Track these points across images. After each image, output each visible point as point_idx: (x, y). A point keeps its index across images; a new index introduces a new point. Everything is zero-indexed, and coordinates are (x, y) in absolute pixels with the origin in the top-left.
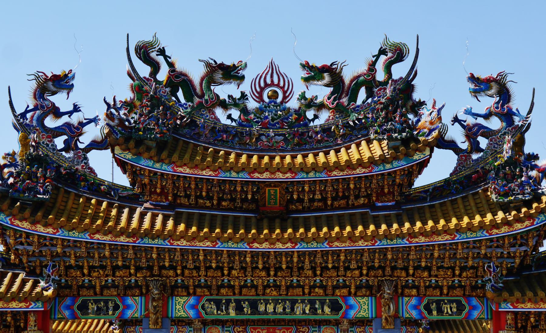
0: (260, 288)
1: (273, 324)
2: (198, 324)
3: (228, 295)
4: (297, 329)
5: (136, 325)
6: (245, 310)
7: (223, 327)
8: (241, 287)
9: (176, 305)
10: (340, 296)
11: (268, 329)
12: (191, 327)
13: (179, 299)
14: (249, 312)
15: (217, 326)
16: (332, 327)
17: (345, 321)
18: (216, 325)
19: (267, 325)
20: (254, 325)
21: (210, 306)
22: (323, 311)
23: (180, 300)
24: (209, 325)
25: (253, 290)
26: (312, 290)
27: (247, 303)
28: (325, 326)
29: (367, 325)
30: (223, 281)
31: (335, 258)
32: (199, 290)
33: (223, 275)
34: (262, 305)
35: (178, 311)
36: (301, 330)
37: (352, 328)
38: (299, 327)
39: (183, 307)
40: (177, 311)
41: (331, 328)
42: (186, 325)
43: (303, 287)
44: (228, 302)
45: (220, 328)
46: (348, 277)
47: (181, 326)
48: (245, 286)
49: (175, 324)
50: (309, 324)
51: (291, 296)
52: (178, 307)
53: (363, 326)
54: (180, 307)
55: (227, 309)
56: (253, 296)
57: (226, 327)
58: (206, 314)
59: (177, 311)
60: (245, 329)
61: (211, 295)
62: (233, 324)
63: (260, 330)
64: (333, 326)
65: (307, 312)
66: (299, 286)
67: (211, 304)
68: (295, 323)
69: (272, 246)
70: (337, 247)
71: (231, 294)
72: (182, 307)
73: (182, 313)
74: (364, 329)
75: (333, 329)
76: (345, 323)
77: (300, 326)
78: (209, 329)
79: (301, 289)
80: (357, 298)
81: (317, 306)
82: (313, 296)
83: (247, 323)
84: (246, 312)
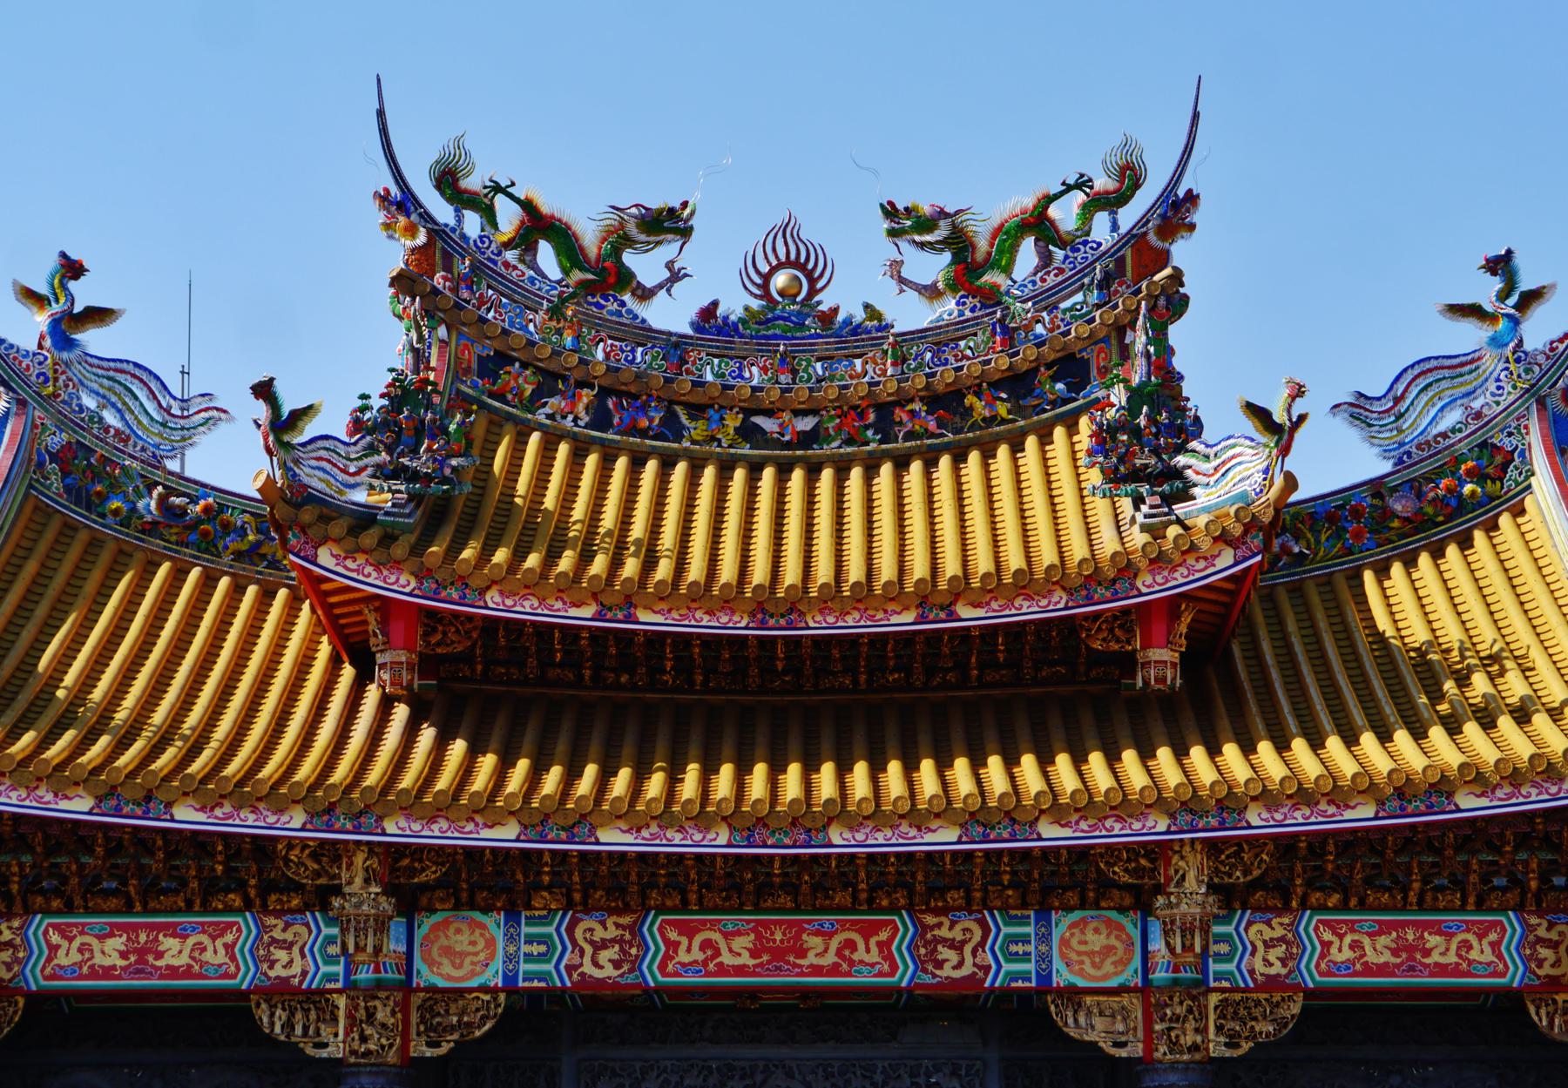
1: (785, 900)
2: (361, 891)
4: (922, 929)
5: (29, 911)
7: (512, 916)
11: (757, 928)
12: (330, 922)
15: (477, 916)
16: (1113, 915)
17: (1191, 875)
18: (473, 906)
19: (757, 910)
20: (684, 907)
24: (433, 911)
28: (1077, 915)
29: (1304, 905)
36: (944, 932)
37: (1226, 920)
38: (930, 920)
41: (1109, 922)
42: (306, 907)
45: (494, 924)
47: (278, 914)
49: (248, 905)
50: (985, 904)
53: (1286, 908)
57: (531, 921)
60: (635, 929)
62: (569, 905)
63: (716, 936)
64: (1122, 910)
68: (911, 896)
74: (1293, 927)
75: (1121, 928)
76: (1191, 883)
77: (937, 912)
78: (435, 928)
83: (644, 896)
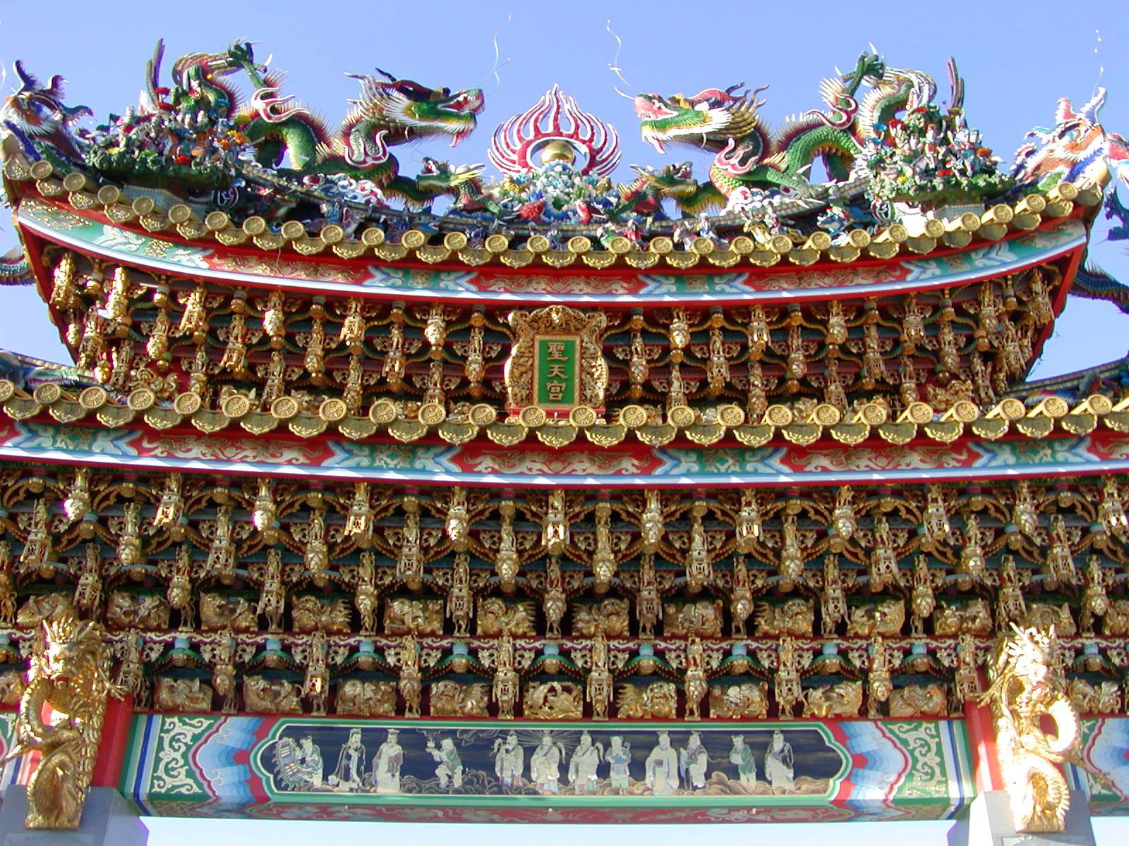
0: (505, 675)
3: (374, 716)
6: (441, 772)
8: (429, 676)
9: (160, 748)
10: (825, 719)
13: (176, 725)
14: (458, 781)
21: (299, 754)
22: (761, 775)
23: (179, 728)
25: (477, 689)
26: (717, 692)
27: (448, 743)
30: (354, 649)
31: (810, 543)
32: (255, 684)
33: (355, 624)
34: (510, 757)
35: (167, 771)
39: (190, 756)
40: (161, 772)
43: (678, 677)
44: (373, 742)
46: (857, 636)
48: (443, 672)
51: (629, 719)
52: (167, 755)
54: (178, 755)
55: (367, 765)
56: (470, 717)
58: (278, 783)
59: (161, 772)
61: (307, 705)
65: (699, 781)
66: (661, 674)
67: (301, 746)
69: (557, 466)
70: (825, 470)
71: (387, 707)
72: (184, 756)
73: (182, 779)
79: (673, 686)
80: (895, 728)
81: (736, 759)
82: (719, 719)
84: (444, 781)
